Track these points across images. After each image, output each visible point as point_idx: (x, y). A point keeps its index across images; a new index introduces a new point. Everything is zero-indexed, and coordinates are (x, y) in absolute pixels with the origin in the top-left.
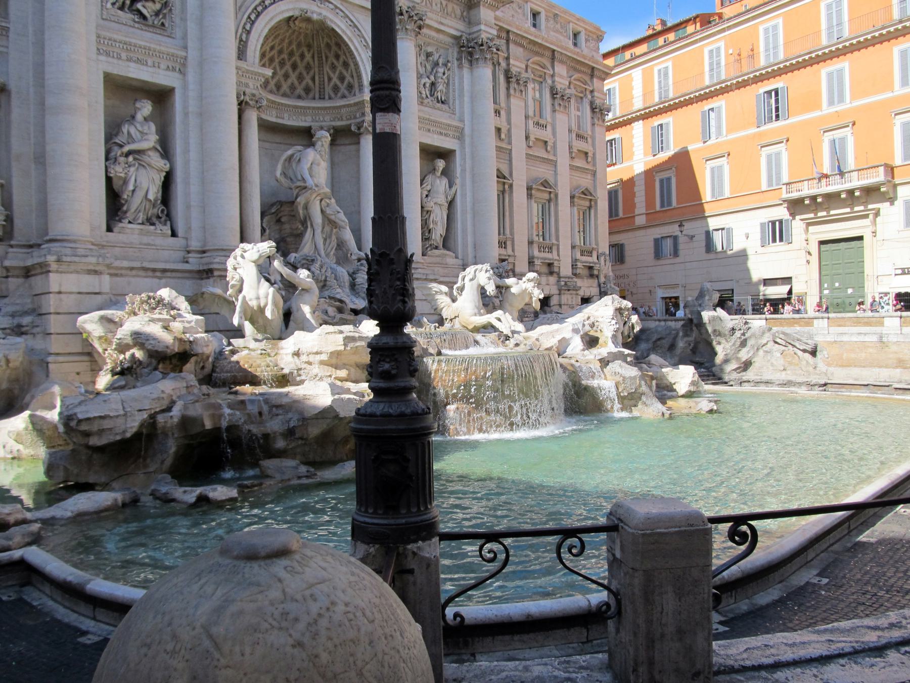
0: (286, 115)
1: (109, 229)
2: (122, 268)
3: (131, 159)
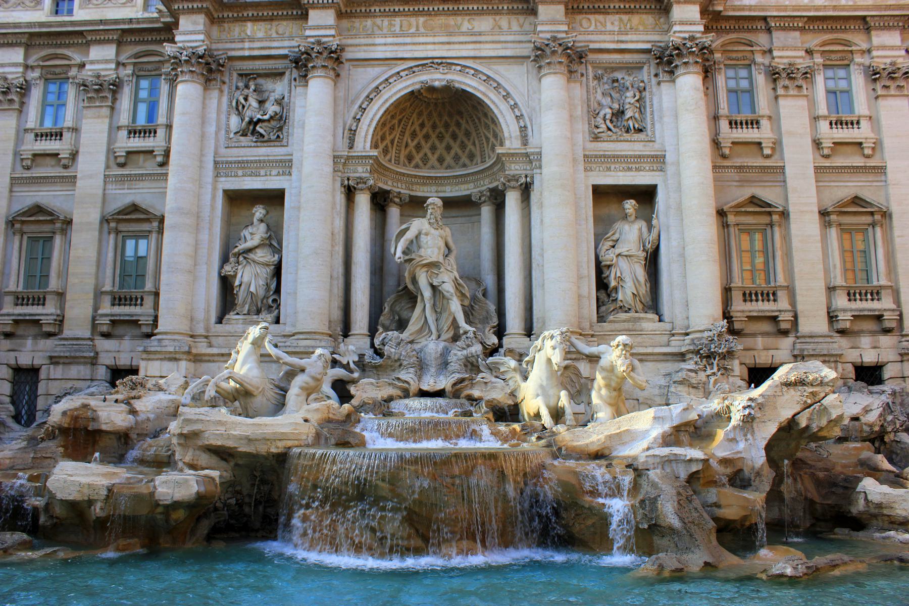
0: (448, 188)
1: (220, 321)
2: (213, 355)
3: (241, 258)
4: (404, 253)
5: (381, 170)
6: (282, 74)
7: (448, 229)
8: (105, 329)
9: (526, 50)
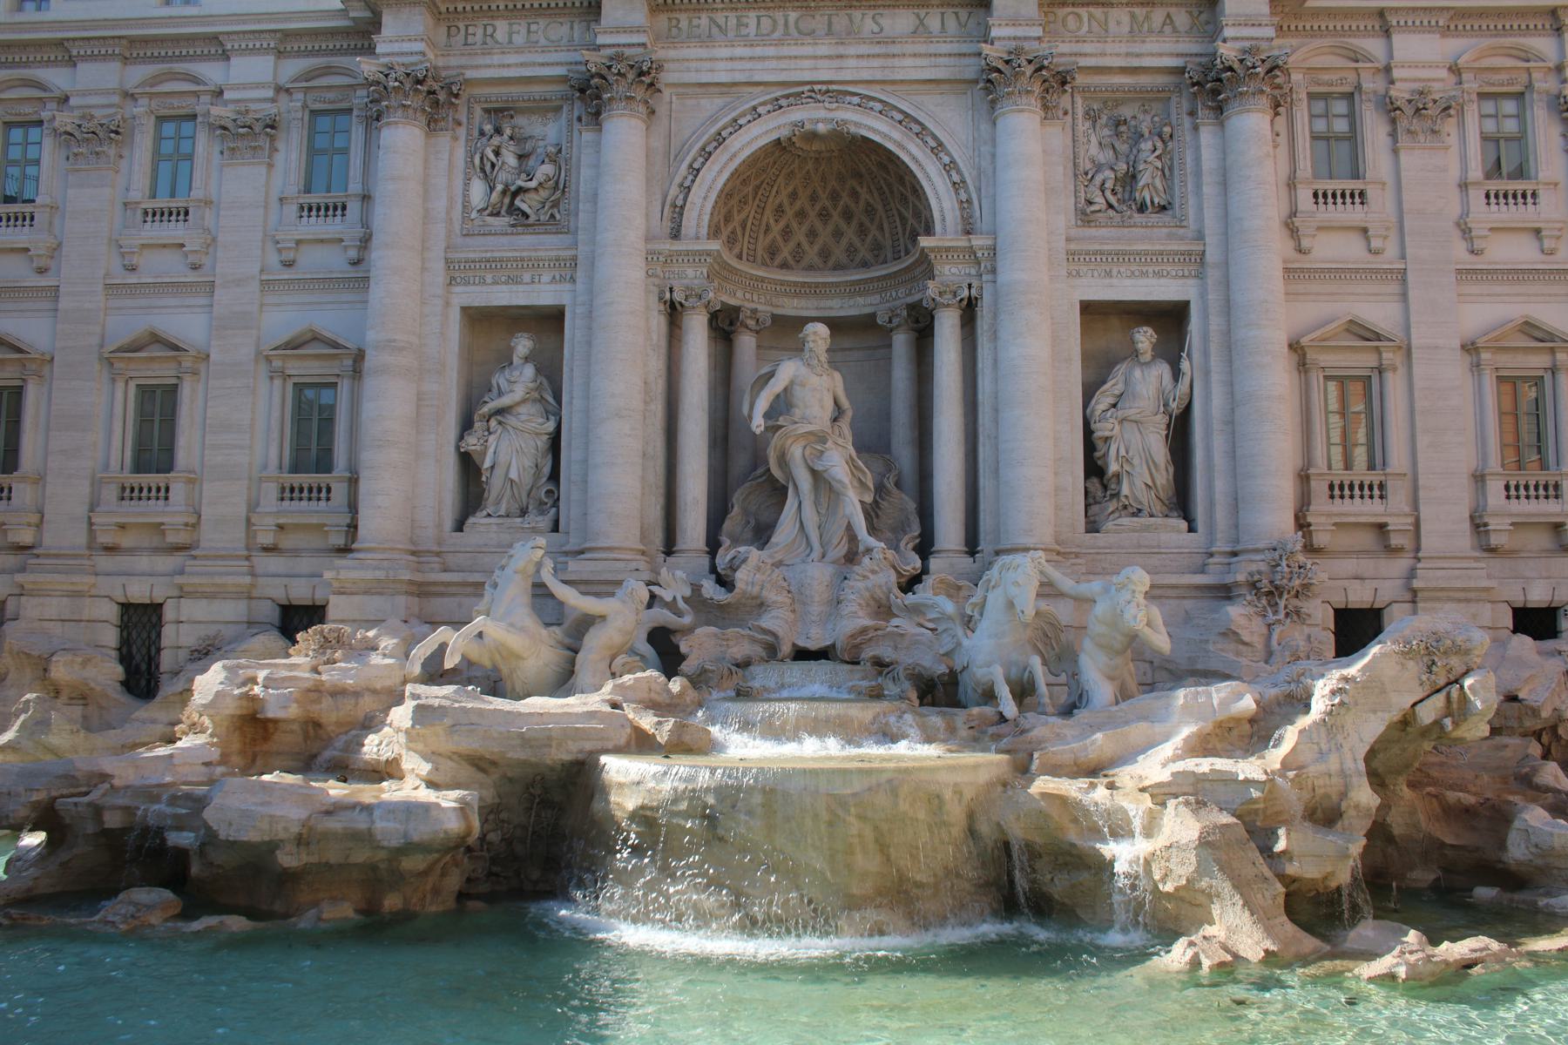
1: (459, 527)
2: (449, 584)
3: (493, 423)
4: (767, 416)
5: (725, 273)
6: (558, 109)
7: (837, 376)
8: (266, 539)
9: (970, 69)
